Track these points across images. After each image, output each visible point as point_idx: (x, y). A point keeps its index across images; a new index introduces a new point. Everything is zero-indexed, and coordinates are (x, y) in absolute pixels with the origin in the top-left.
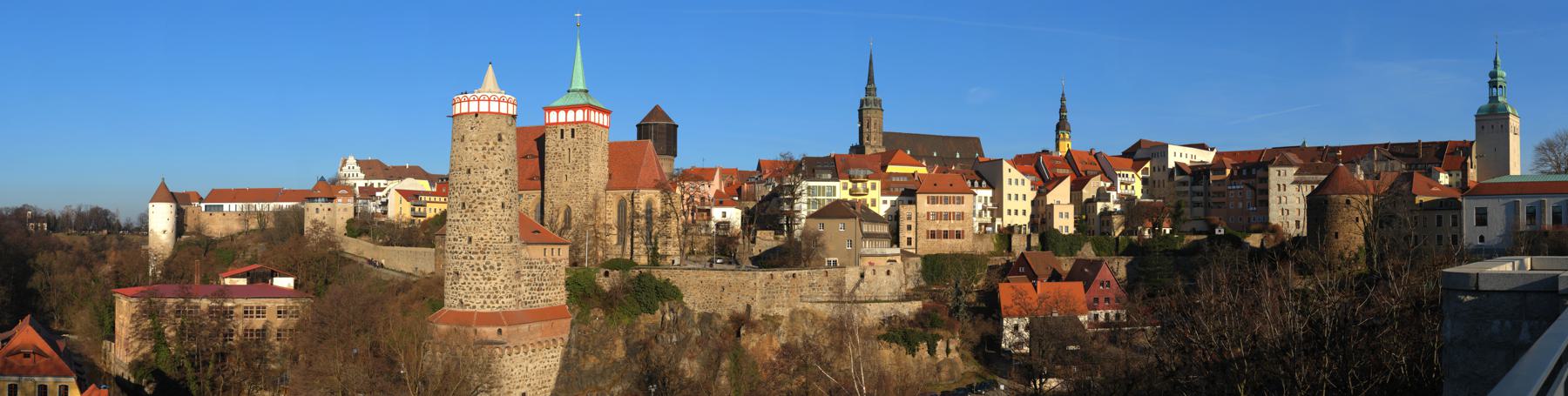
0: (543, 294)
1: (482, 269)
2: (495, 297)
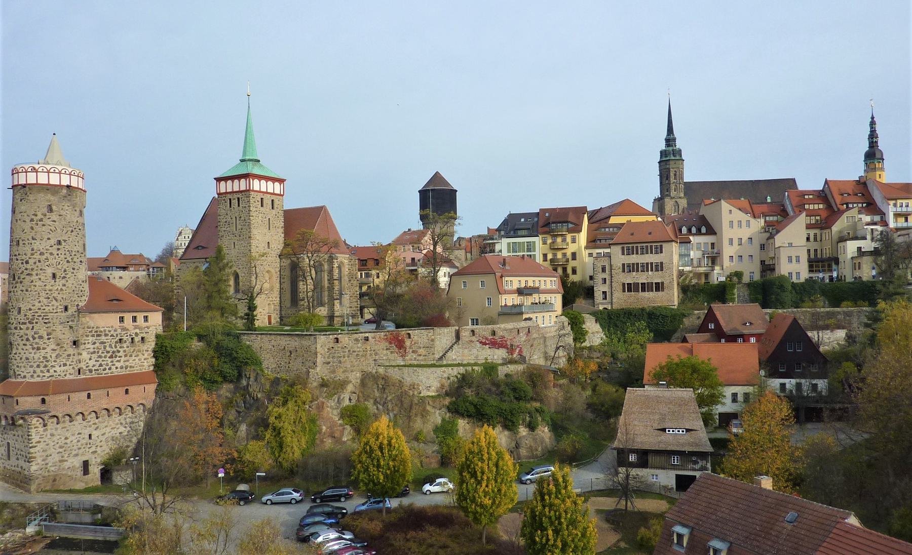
0: (119, 361)
1: (31, 339)
2: (46, 366)
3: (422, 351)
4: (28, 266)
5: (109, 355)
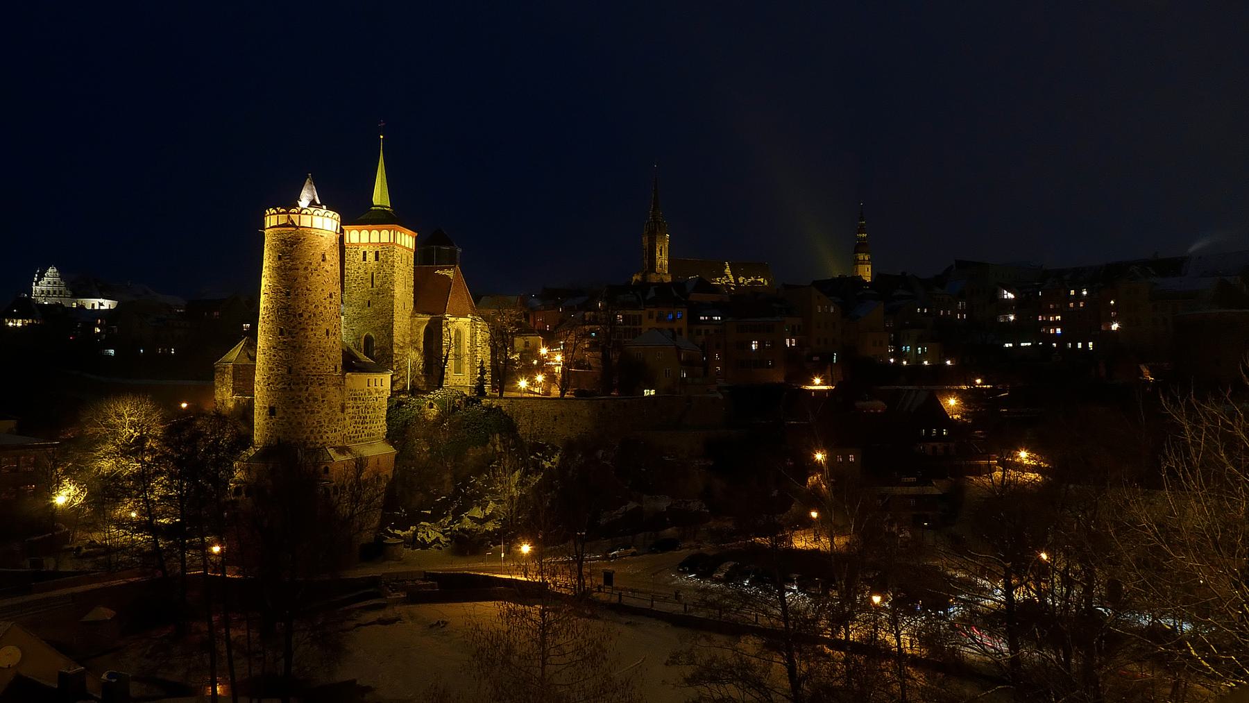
0: (366, 428)
2: (319, 432)
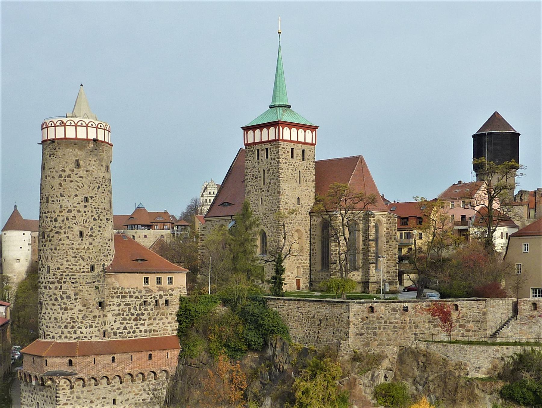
0: (143, 324)
1: (59, 299)
2: (73, 327)
3: (471, 326)
4: (57, 224)
5: (133, 317)
